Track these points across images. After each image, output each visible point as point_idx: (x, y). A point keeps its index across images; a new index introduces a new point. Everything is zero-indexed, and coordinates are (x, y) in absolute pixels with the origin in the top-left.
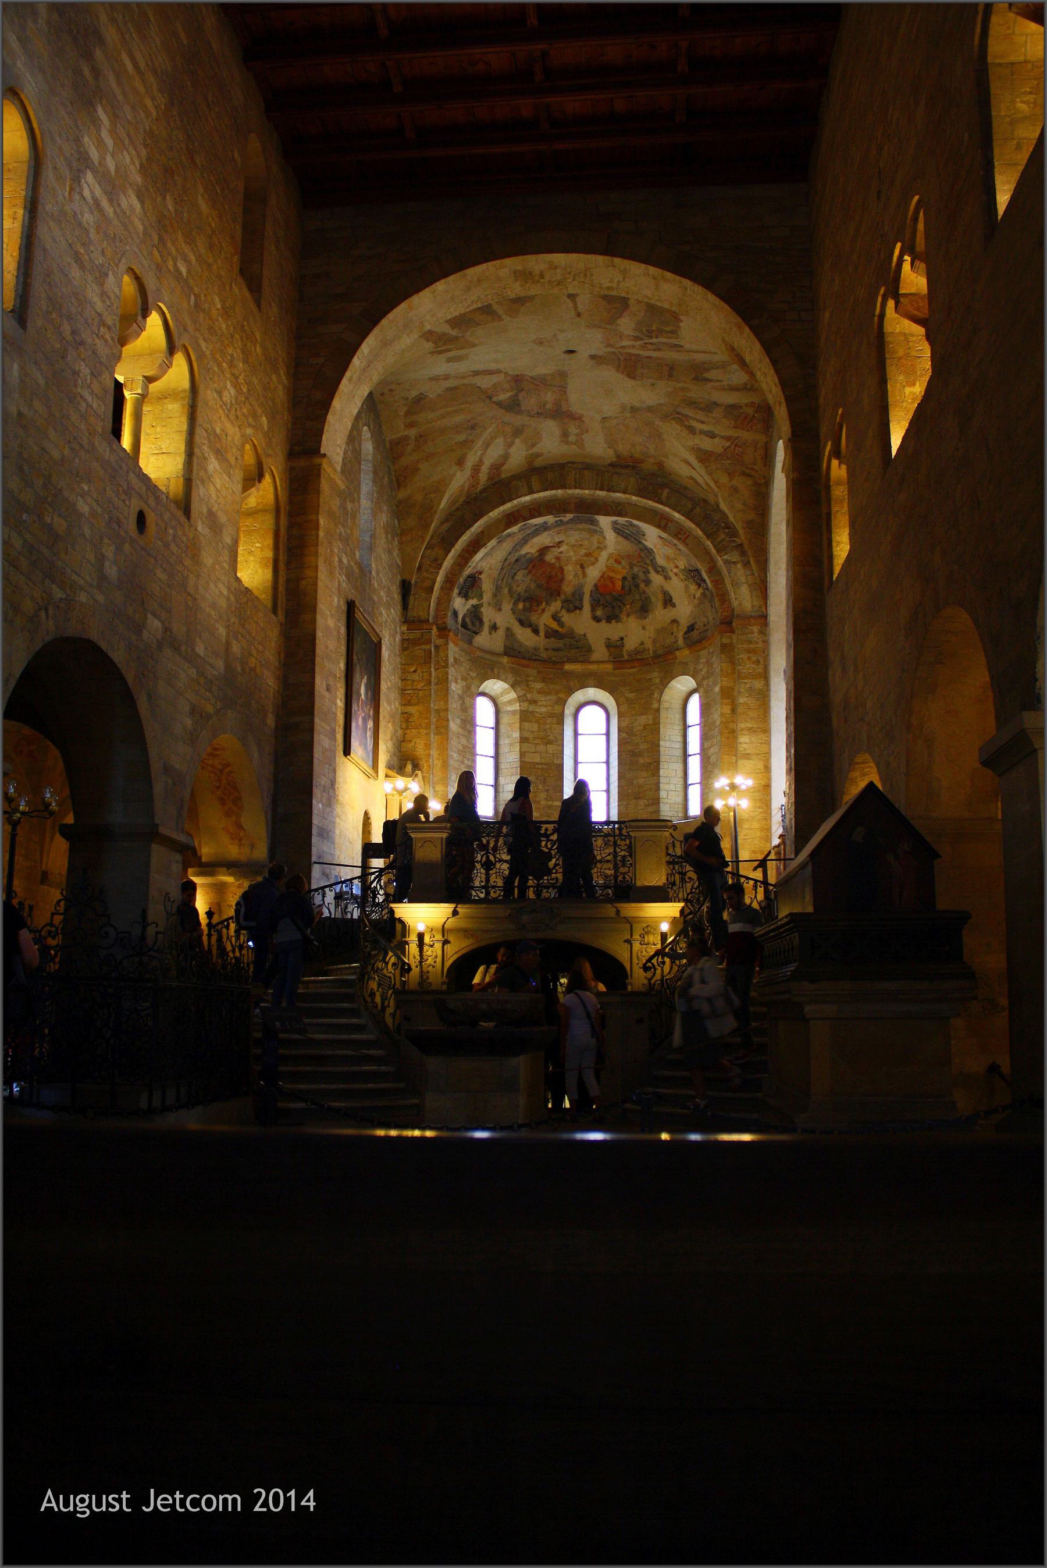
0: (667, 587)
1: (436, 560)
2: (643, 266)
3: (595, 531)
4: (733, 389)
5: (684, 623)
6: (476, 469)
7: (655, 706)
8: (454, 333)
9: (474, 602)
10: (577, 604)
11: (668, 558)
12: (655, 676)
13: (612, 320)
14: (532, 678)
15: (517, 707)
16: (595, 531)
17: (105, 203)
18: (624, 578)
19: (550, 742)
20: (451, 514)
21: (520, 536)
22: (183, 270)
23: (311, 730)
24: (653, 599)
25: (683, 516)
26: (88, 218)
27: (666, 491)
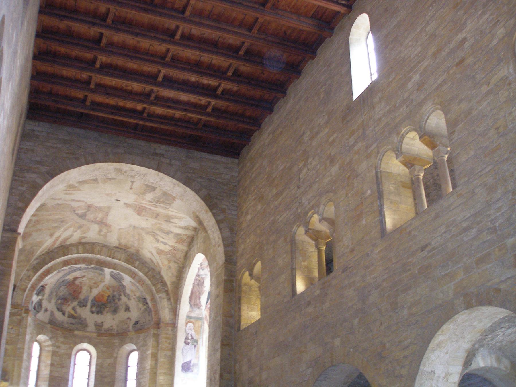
0: (129, 303)
1: (29, 277)
2: (171, 178)
3: (102, 274)
5: (134, 320)
6: (57, 239)
7: (115, 355)
8: (76, 185)
9: (40, 297)
10: (85, 304)
11: (132, 291)
12: (116, 341)
13: (144, 193)
14: (59, 336)
15: (51, 349)
16: (102, 274)
18: (109, 296)
19: (64, 367)
20: (40, 257)
21: (68, 271)
24: (120, 307)
25: (144, 274)
27: (138, 263)
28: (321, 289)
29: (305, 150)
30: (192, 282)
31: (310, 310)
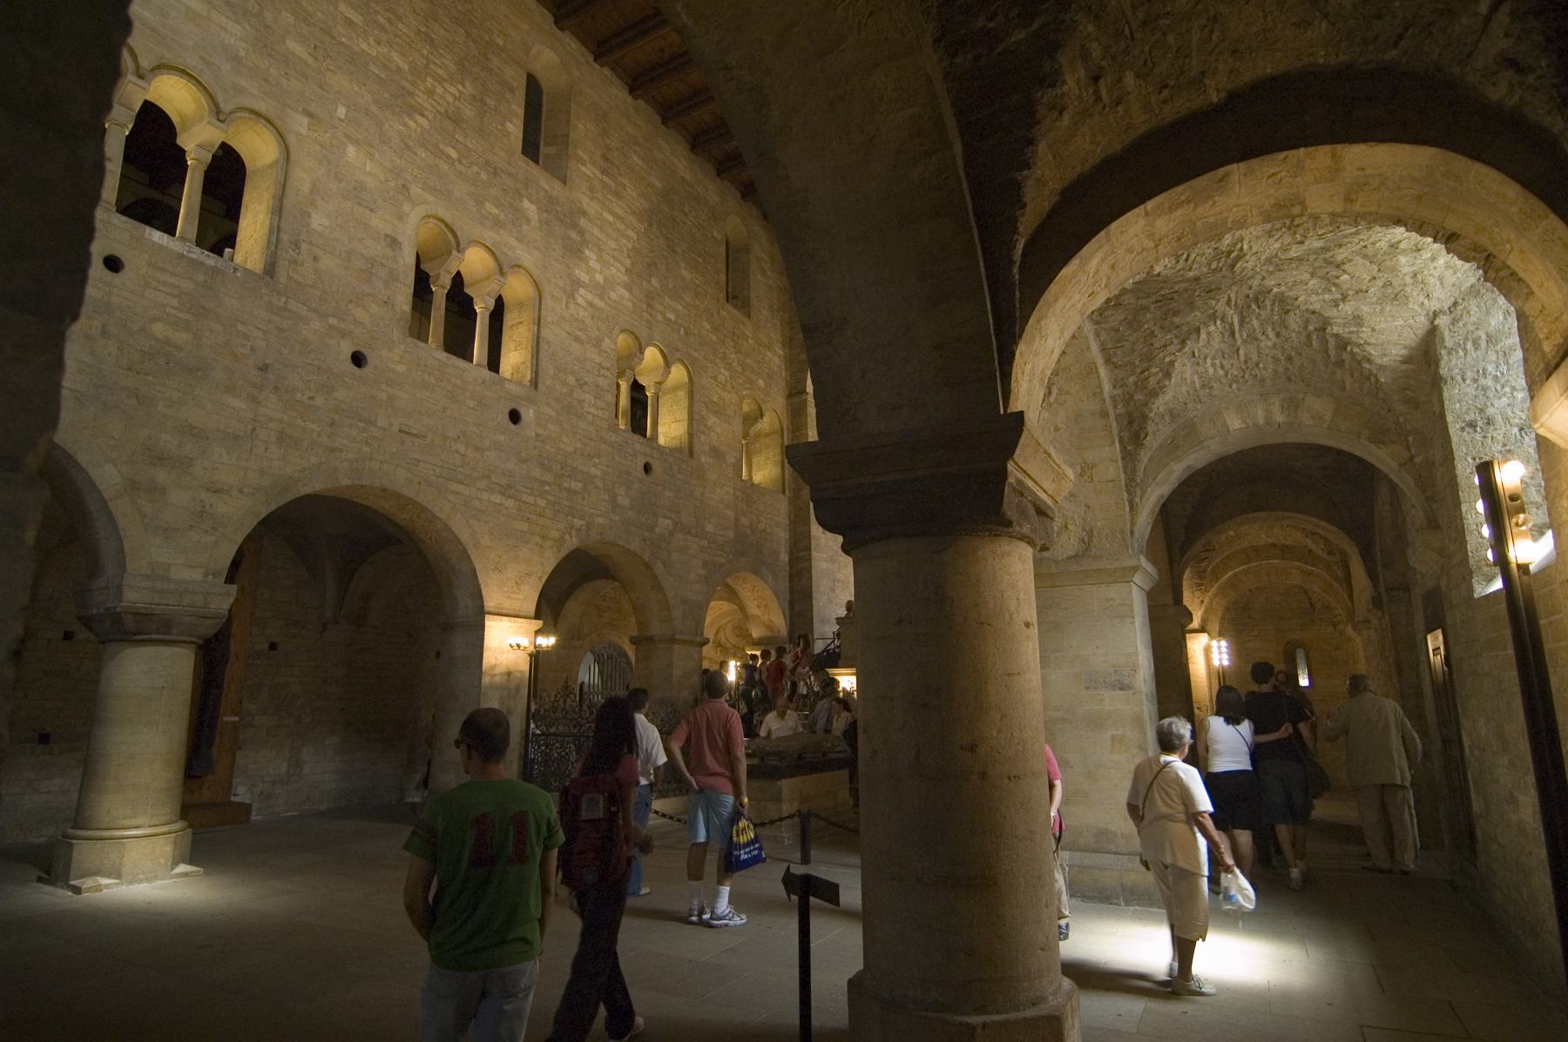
17: (597, 302)
22: (672, 316)
23: (810, 559)
26: (582, 314)
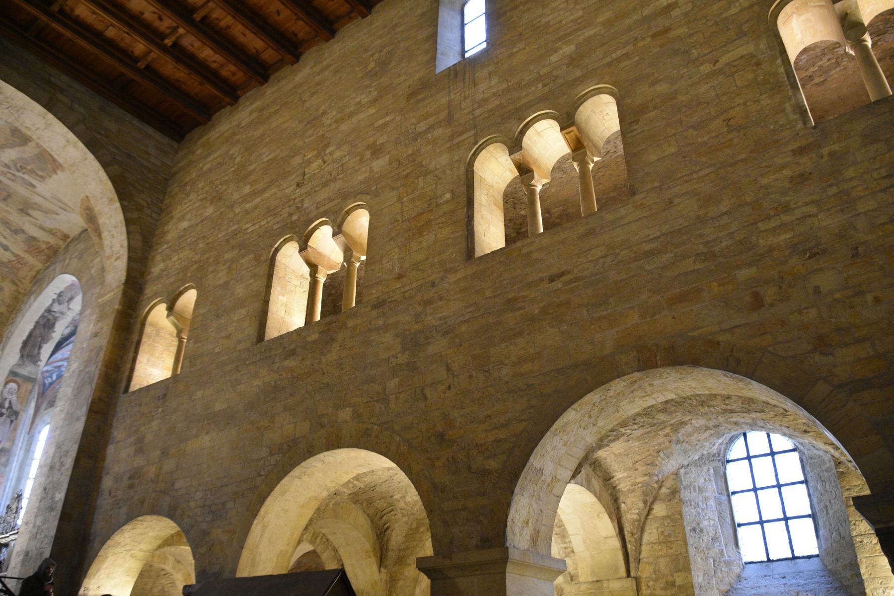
2: (66, 129)
4: (42, 228)
28: (320, 333)
29: (323, 135)
30: (36, 318)
31: (291, 363)
